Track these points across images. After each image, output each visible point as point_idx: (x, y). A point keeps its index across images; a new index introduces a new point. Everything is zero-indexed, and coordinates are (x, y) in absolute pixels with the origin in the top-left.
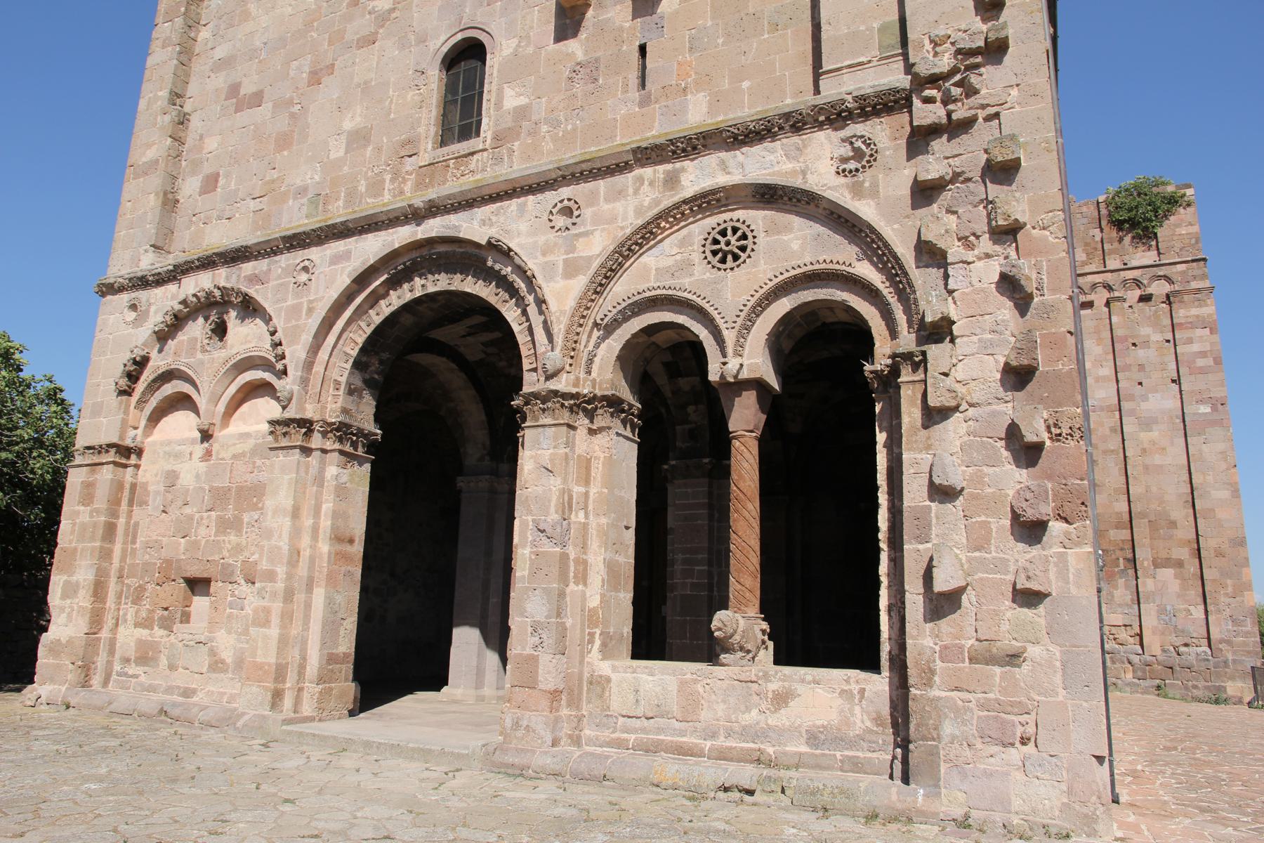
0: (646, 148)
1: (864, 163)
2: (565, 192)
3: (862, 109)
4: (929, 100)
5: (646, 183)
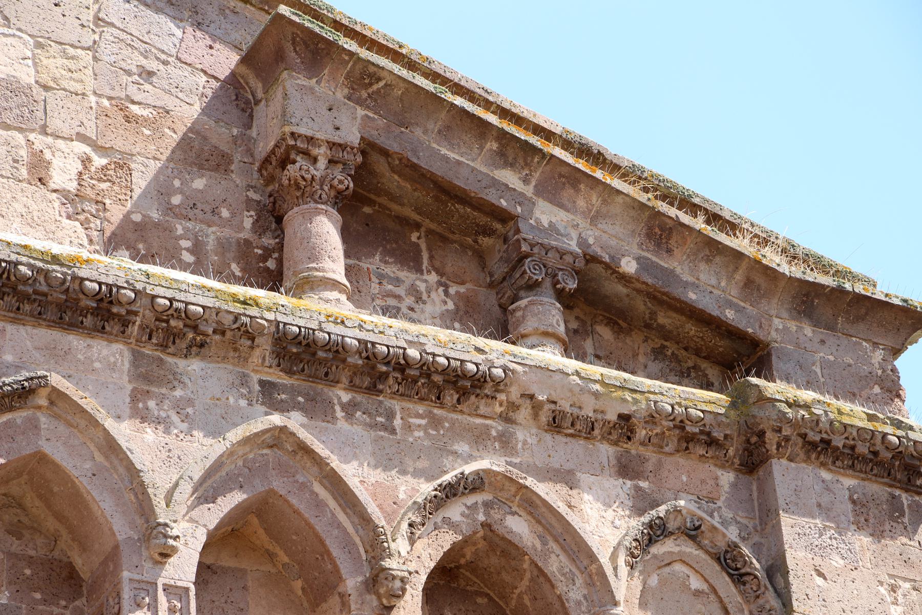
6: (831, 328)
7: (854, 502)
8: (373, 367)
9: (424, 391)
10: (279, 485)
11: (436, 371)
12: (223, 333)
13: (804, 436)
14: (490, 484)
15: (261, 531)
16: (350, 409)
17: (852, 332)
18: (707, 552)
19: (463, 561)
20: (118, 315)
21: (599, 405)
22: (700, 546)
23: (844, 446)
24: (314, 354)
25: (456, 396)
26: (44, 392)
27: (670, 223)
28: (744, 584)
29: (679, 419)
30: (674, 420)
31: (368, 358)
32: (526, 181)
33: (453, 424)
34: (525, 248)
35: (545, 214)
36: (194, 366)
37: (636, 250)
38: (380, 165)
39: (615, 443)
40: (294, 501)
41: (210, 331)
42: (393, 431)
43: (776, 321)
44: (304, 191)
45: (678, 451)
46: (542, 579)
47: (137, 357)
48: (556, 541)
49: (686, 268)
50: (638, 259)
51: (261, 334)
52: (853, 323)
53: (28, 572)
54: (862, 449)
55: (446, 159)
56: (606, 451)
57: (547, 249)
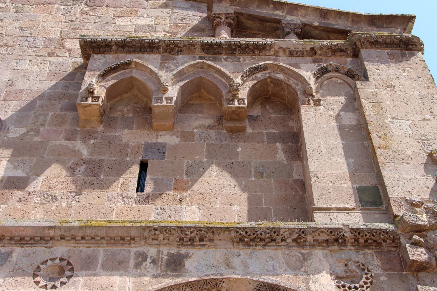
0: (155, 230)
1: (362, 283)
2: (60, 250)
3: (357, 240)
4: (416, 244)
5: (149, 260)
6: (382, 27)
7: (389, 55)
8: (232, 48)
9: (248, 52)
10: (203, 75)
11: (250, 46)
12: (186, 46)
13: (368, 41)
14: (270, 67)
15: (206, 93)
16: (226, 59)
17: (389, 27)
18: (343, 74)
19: (270, 93)
20: (156, 47)
21: (304, 47)
22: (340, 73)
23: (382, 41)
24: (213, 47)
25: (259, 52)
26: (133, 63)
27: (326, 11)
28: (354, 78)
29: (329, 46)
30: (328, 47)
31: (229, 45)
32: (283, 12)
33: (259, 58)
34: (283, 25)
35: (289, 18)
36: (180, 56)
37: (318, 21)
38: (243, 19)
39: (312, 57)
40: (207, 78)
41: (182, 46)
42: (240, 62)
43: (364, 28)
44: (219, 24)
45: (332, 55)
46: (289, 87)
47: (162, 57)
48: (292, 77)
49: (334, 22)
50: (319, 22)
51: (197, 44)
52: (389, 24)
53: (138, 110)
54: (389, 41)
55: (260, 12)
56: (309, 59)
57: (290, 24)
